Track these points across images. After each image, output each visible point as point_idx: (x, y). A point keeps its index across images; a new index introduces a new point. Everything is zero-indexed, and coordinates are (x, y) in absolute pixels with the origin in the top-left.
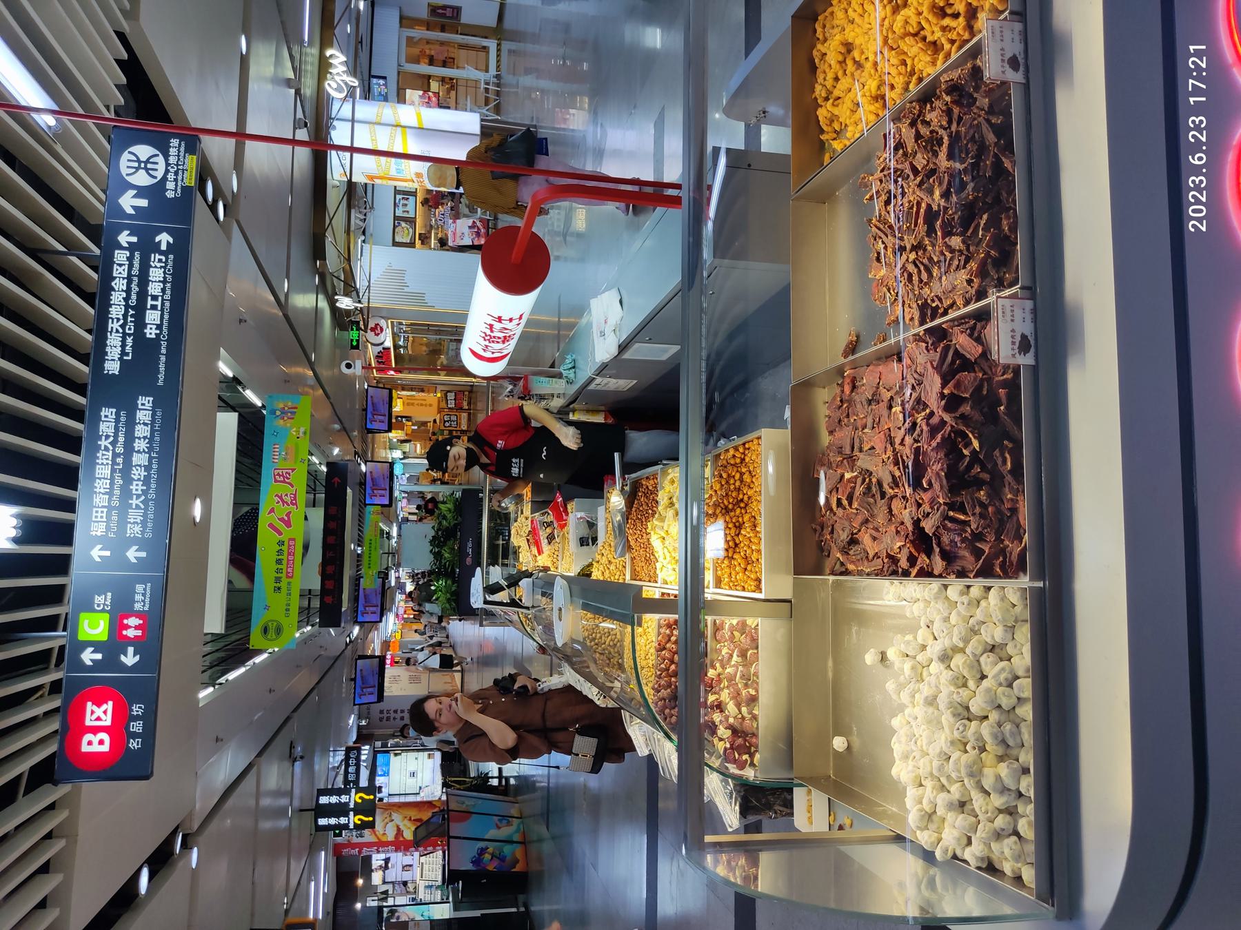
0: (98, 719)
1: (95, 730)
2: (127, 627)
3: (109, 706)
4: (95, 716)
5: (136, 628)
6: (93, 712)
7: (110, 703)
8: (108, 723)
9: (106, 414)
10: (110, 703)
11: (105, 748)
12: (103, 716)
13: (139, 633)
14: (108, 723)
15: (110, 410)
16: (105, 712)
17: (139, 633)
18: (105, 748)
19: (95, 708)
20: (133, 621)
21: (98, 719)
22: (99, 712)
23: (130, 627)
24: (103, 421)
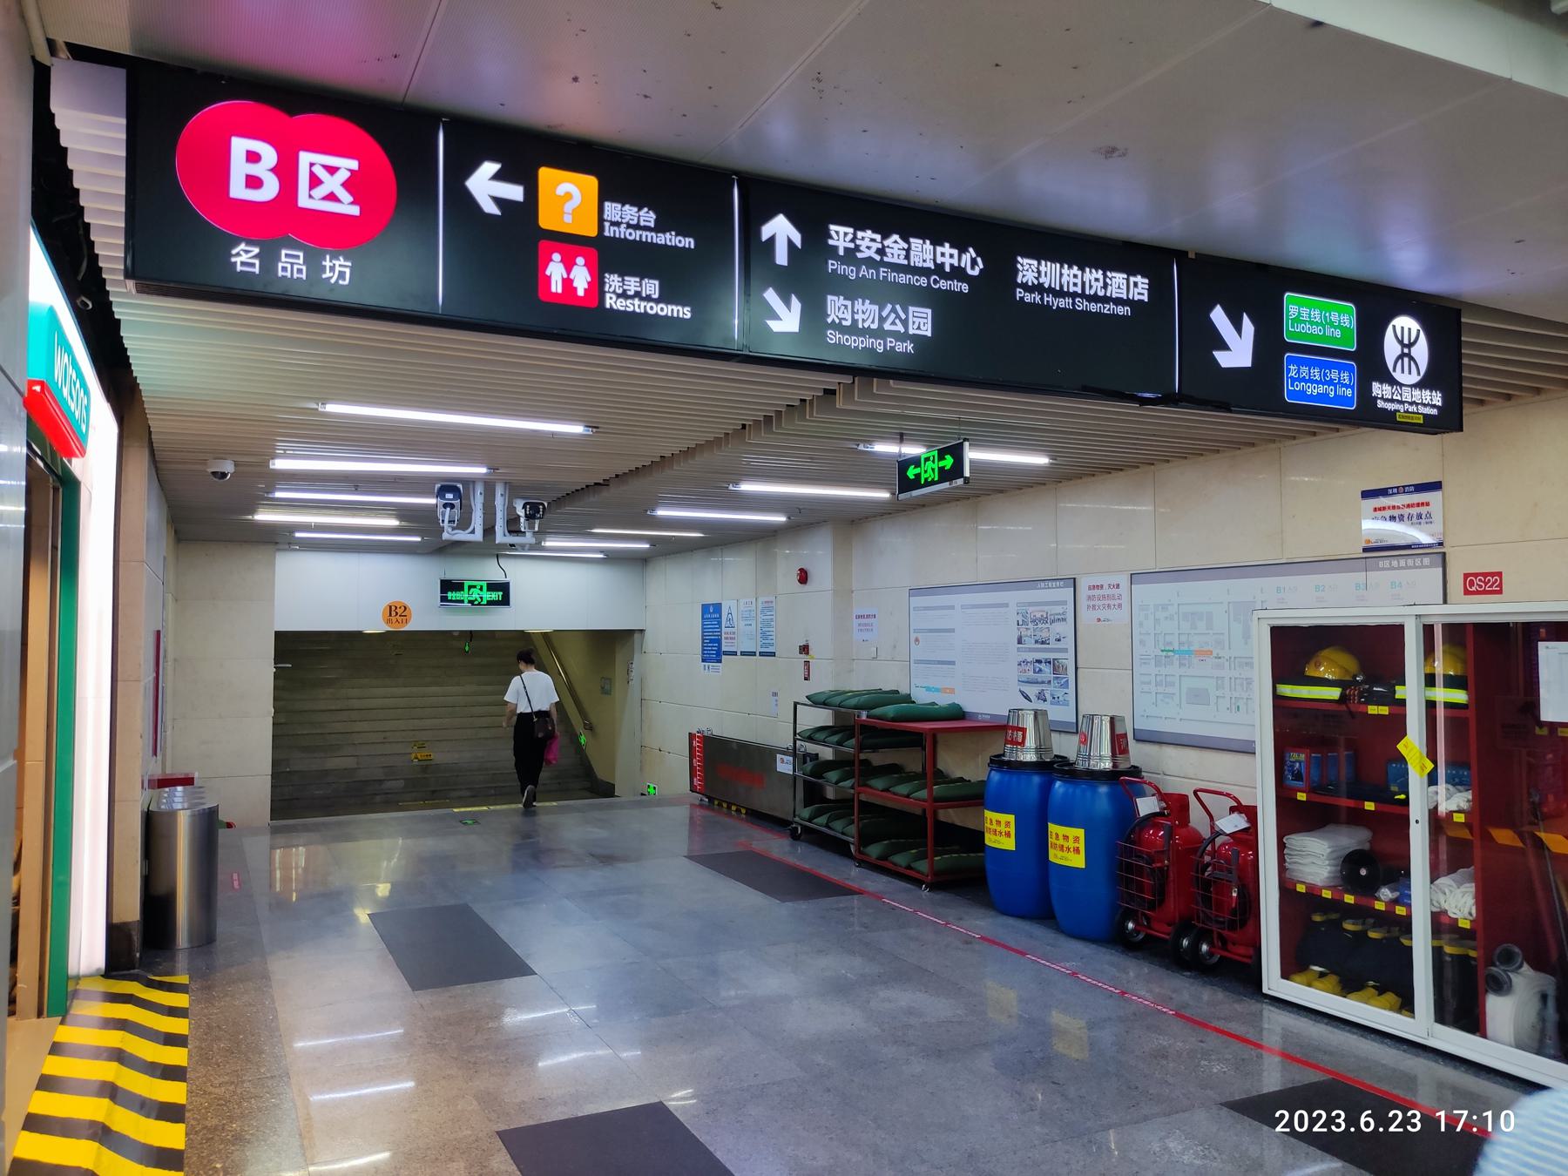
0: (315, 181)
1: (286, 171)
2: (569, 265)
3: (347, 206)
4: (321, 173)
5: (568, 283)
6: (332, 170)
7: (355, 211)
8: (304, 201)
9: (1140, 285)
10: (355, 211)
11: (238, 190)
12: (320, 192)
13: (556, 287)
14: (304, 201)
15: (1146, 292)
16: (332, 197)
17: (556, 287)
18: (238, 190)
19: (343, 175)
20: (581, 278)
21: (315, 181)
22: (333, 184)
23: (569, 270)
24: (1128, 280)
